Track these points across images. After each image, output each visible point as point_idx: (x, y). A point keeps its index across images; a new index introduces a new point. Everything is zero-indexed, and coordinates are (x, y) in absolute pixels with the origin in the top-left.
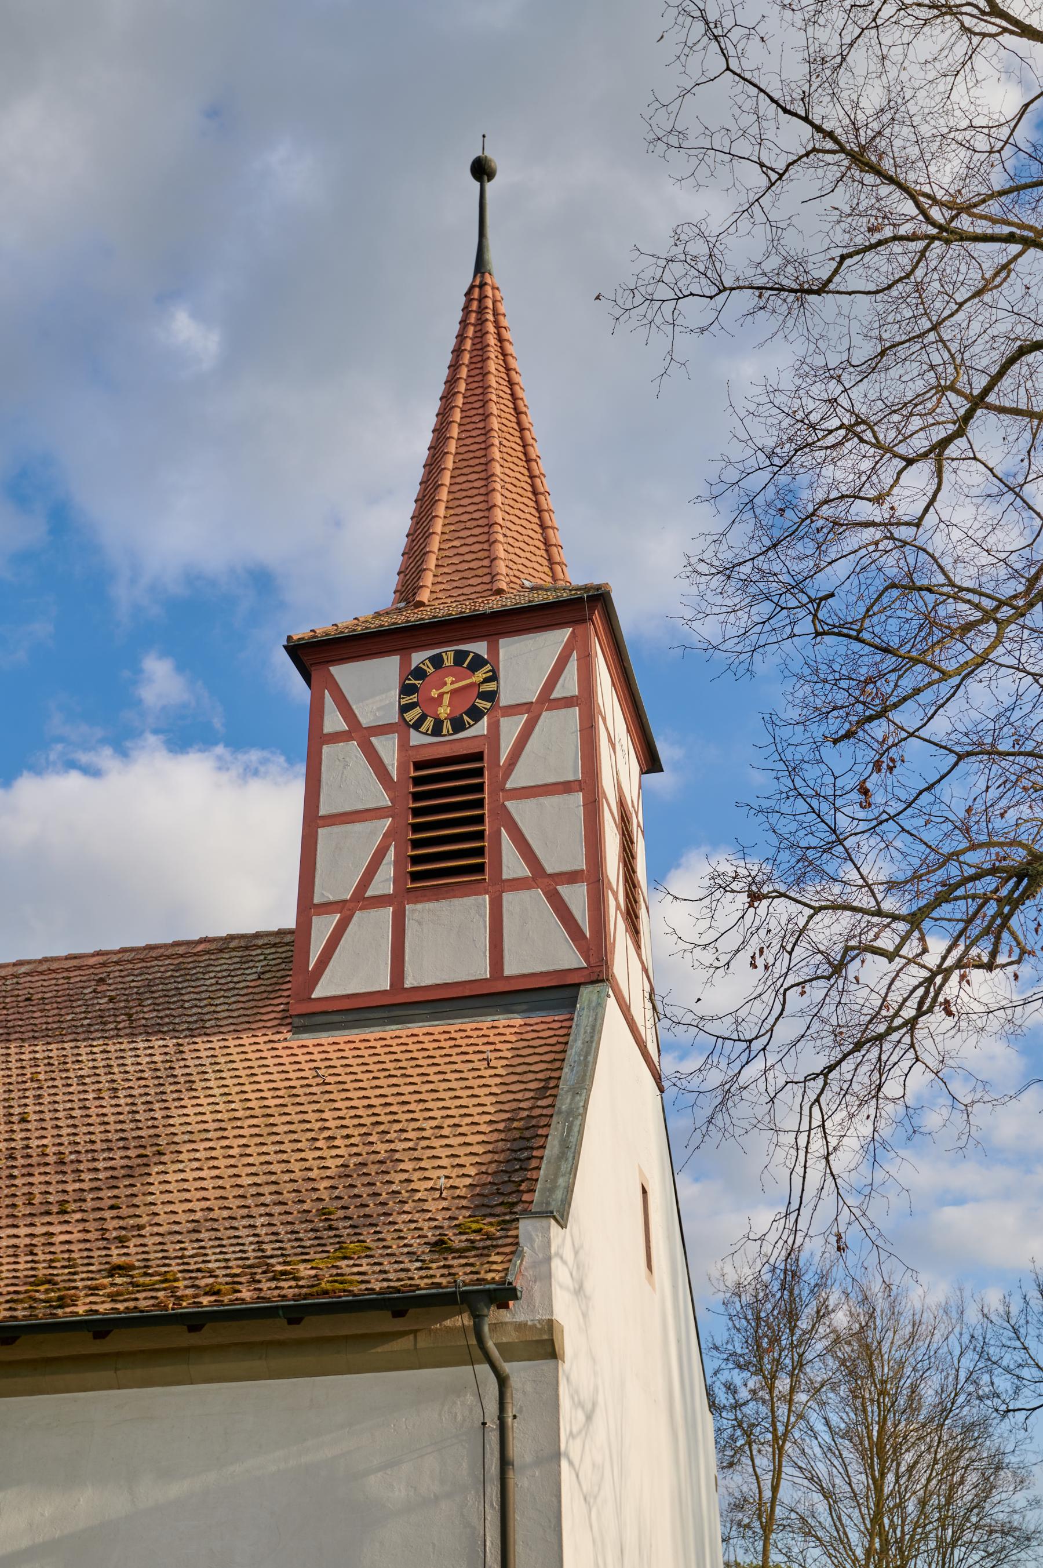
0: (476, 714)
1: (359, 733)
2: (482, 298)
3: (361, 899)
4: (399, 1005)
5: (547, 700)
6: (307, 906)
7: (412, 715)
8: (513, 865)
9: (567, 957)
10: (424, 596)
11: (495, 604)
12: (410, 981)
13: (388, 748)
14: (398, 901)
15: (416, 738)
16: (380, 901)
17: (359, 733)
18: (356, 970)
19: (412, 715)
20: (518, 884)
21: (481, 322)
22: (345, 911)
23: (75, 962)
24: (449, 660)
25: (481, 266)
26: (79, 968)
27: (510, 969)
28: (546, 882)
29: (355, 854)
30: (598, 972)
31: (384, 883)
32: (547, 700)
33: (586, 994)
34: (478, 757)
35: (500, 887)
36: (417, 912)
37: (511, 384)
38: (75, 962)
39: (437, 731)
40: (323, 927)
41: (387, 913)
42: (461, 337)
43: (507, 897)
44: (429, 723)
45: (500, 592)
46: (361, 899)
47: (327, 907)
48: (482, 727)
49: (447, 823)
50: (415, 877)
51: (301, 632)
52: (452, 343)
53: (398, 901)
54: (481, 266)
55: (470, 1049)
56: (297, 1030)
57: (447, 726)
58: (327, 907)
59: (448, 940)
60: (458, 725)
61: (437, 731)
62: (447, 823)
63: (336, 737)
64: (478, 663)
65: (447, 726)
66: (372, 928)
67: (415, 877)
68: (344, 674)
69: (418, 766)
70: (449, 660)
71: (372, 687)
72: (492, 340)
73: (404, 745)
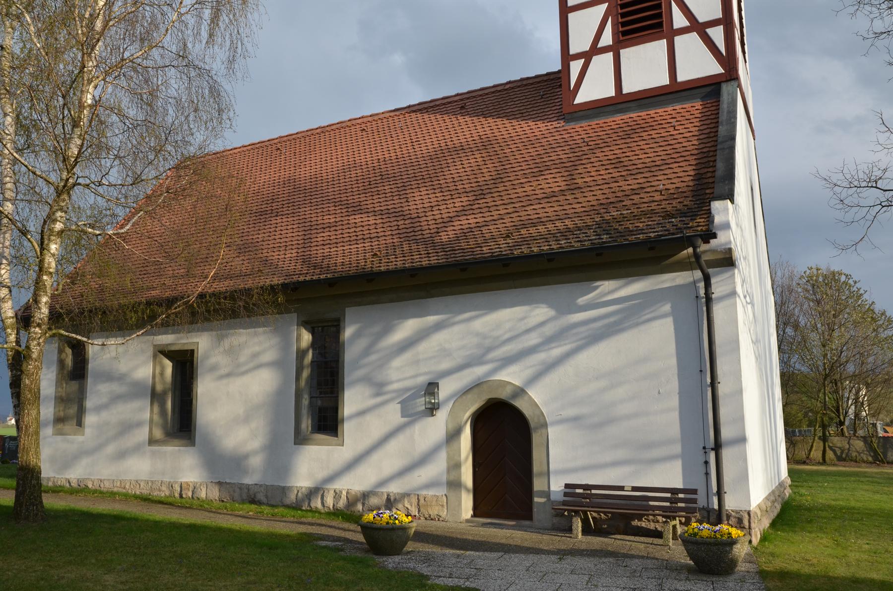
3: (595, 50)
4: (622, 102)
6: (567, 57)
8: (679, 20)
9: (714, 68)
12: (625, 90)
14: (615, 49)
18: (596, 86)
20: (683, 31)
22: (587, 57)
23: (446, 101)
26: (450, 103)
27: (681, 77)
28: (699, 27)
30: (731, 74)
31: (607, 39)
33: (726, 88)
35: (671, 35)
36: (626, 54)
38: (446, 101)
40: (576, 67)
41: (610, 55)
43: (677, 39)
46: (595, 50)
47: (577, 56)
50: (624, 33)
55: (663, 122)
56: (567, 121)
58: (577, 56)
59: (646, 66)
66: (603, 64)
67: (624, 33)
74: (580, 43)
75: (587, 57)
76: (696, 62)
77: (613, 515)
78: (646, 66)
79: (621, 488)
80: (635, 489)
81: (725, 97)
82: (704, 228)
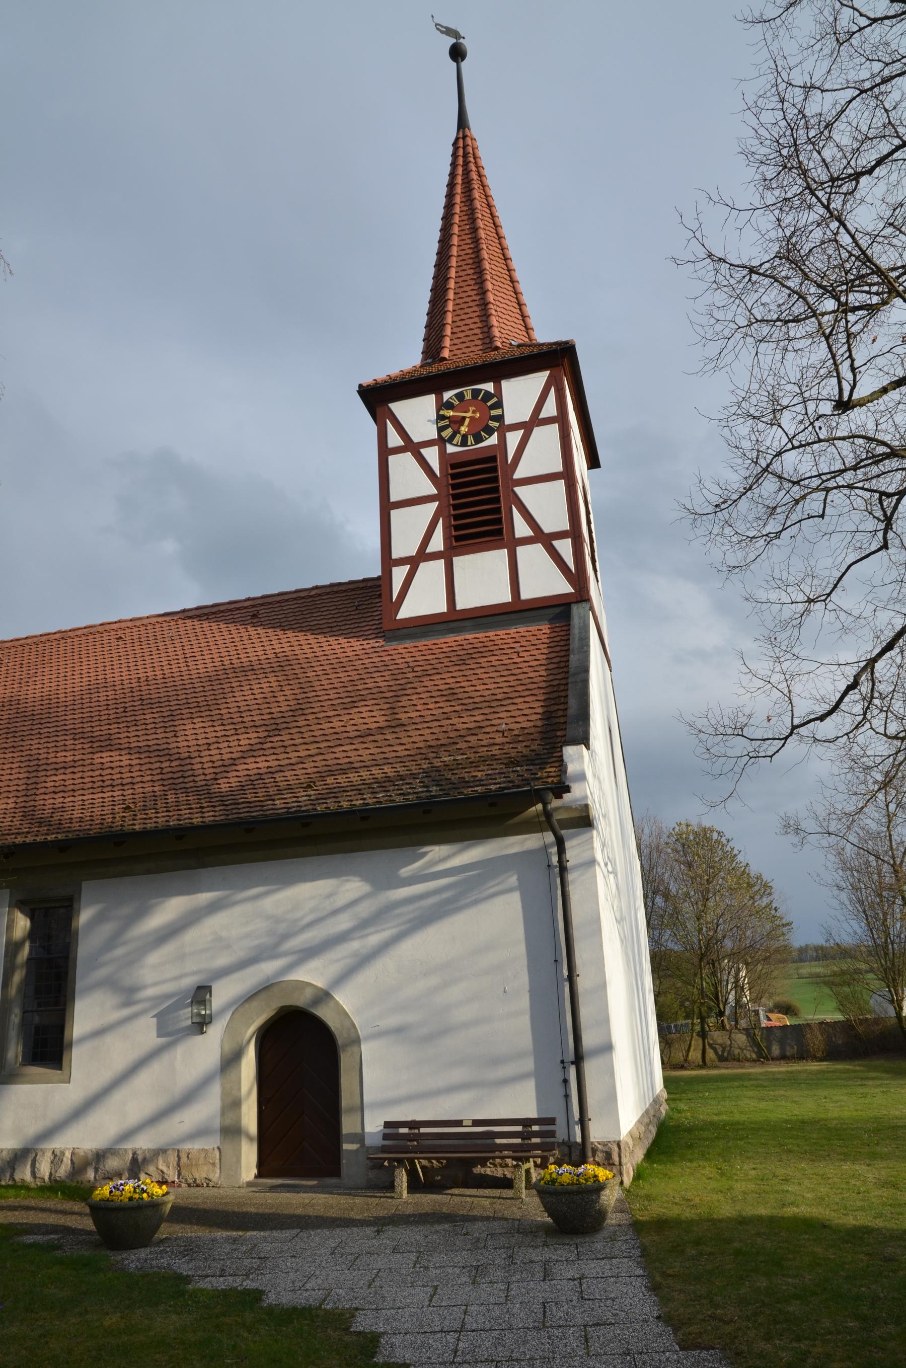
0: (490, 431)
1: (413, 447)
2: (465, 147)
5: (536, 421)
6: (388, 562)
7: (447, 433)
8: (522, 529)
9: (564, 587)
10: (446, 354)
11: (494, 356)
12: (460, 606)
13: (432, 455)
14: (447, 555)
15: (450, 449)
16: (435, 556)
17: (413, 447)
18: (423, 598)
19: (447, 433)
21: (466, 164)
22: (414, 562)
23: (233, 606)
24: (468, 396)
25: (462, 122)
26: (238, 609)
27: (525, 595)
28: (545, 539)
29: (411, 528)
31: (437, 543)
32: (536, 421)
33: (576, 610)
34: (493, 459)
35: (513, 545)
36: (460, 562)
37: (490, 206)
38: (233, 606)
39: (464, 443)
40: (399, 574)
41: (441, 563)
42: (453, 175)
43: (520, 550)
44: (458, 438)
45: (497, 348)
47: (401, 562)
48: (493, 440)
49: (476, 504)
50: (458, 539)
51: (367, 380)
52: (446, 179)
53: (447, 555)
54: (462, 122)
55: (505, 646)
57: (470, 439)
58: (401, 562)
59: (483, 579)
60: (478, 439)
61: (464, 443)
62: (476, 504)
63: (397, 450)
64: (488, 396)
65: (470, 439)
66: (431, 573)
67: (458, 539)
68: (401, 409)
69: (453, 466)
70: (468, 396)
71: (418, 415)
72: (474, 176)
73: (442, 453)
74: (404, 546)
75: (414, 562)
76: (542, 579)
77: (447, 1160)
78: (483, 579)
79: (459, 1123)
80: (476, 1123)
81: (576, 621)
82: (555, 780)
